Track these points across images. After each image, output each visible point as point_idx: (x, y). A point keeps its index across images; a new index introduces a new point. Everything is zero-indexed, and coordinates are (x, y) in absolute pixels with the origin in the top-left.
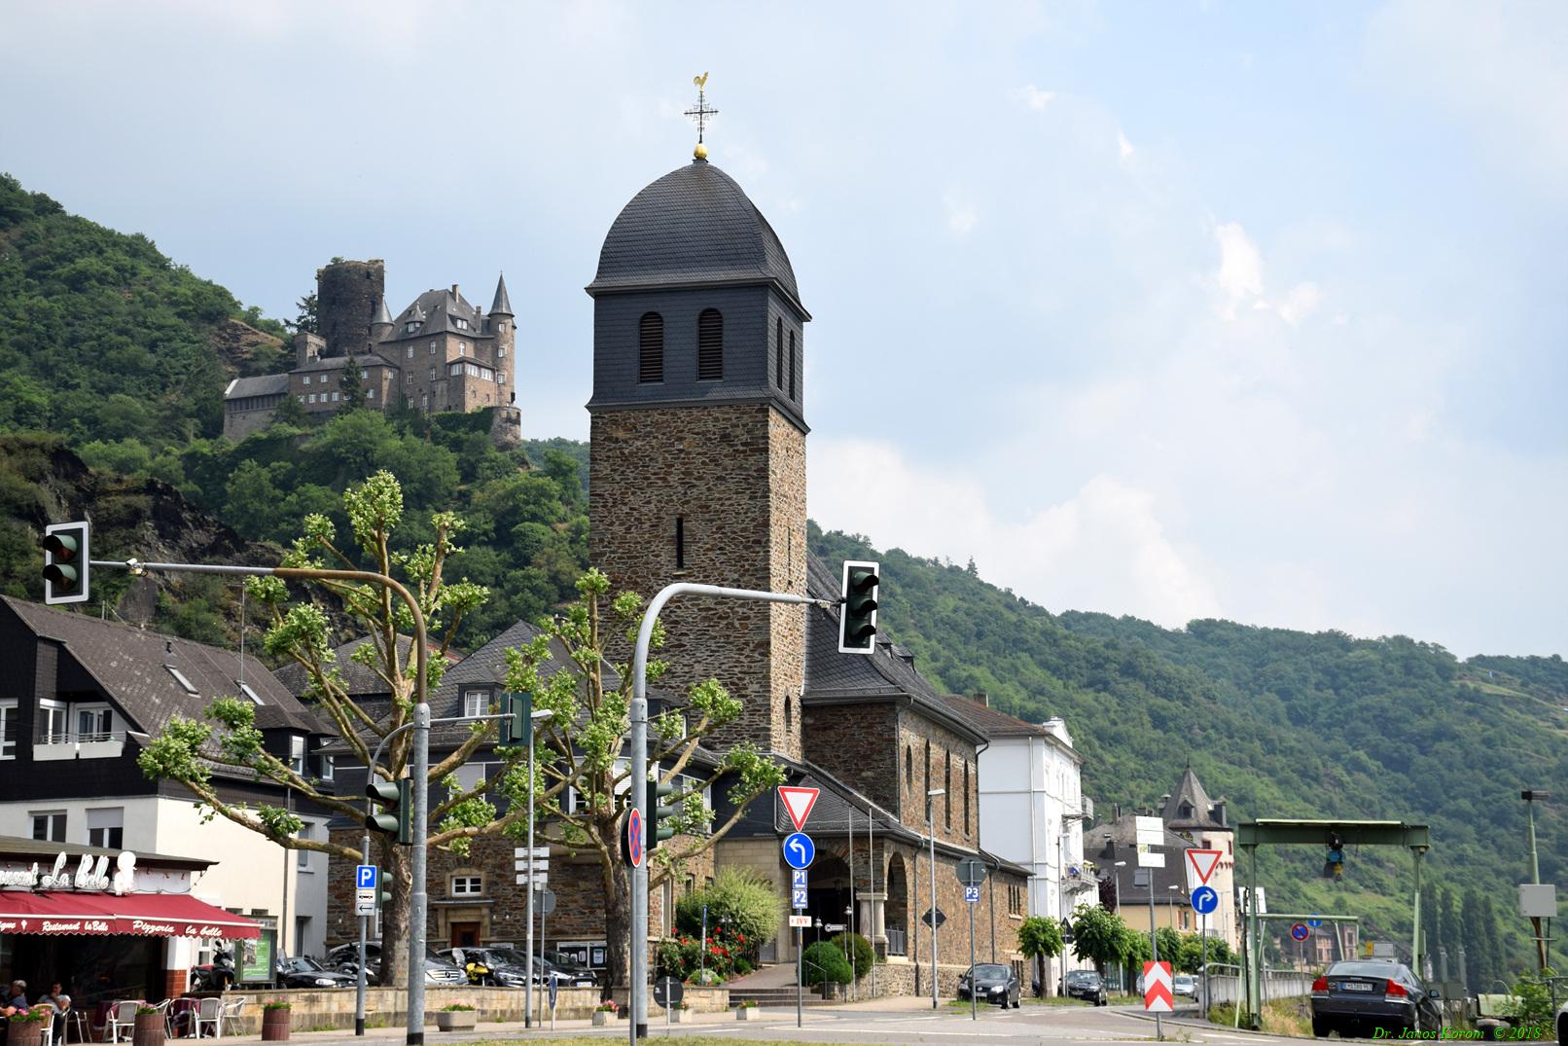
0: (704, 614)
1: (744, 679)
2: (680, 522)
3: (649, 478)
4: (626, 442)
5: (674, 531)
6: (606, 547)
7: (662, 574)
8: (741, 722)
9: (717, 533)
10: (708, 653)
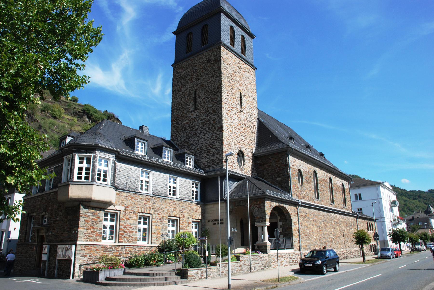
0: (202, 121)
1: (214, 142)
2: (195, 92)
3: (187, 81)
4: (181, 72)
5: (193, 96)
6: (176, 107)
7: (190, 111)
8: (214, 158)
10: (203, 135)
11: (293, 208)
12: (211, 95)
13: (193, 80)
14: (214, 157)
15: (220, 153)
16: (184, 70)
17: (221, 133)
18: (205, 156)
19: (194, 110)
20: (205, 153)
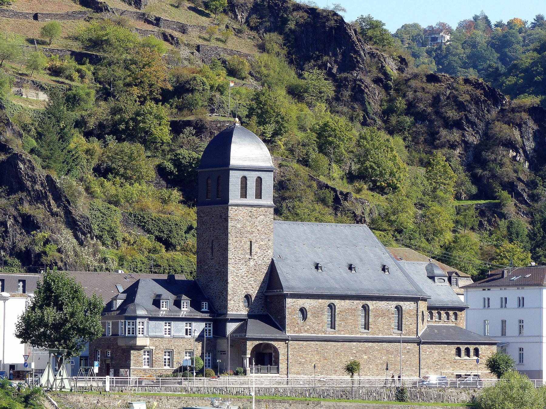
11: (283, 343)
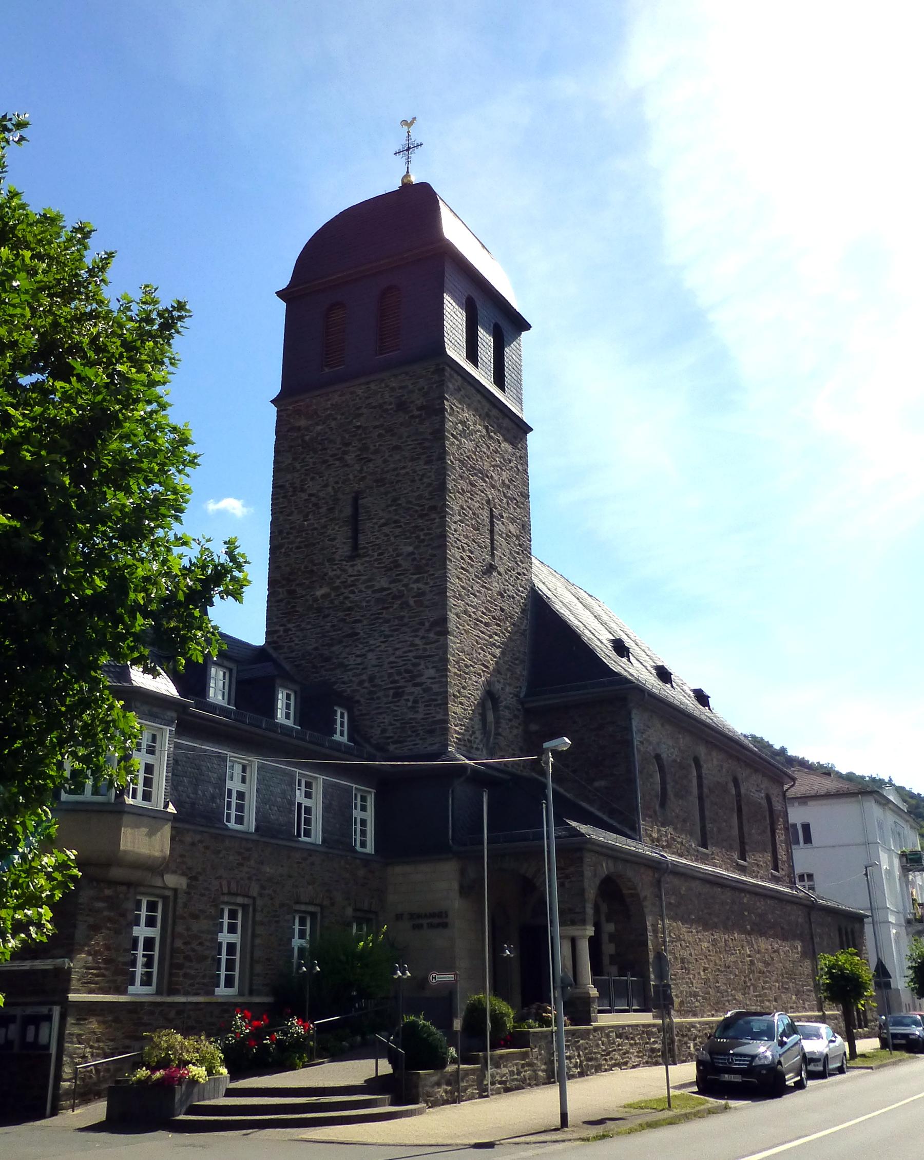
0: (378, 595)
1: (419, 664)
2: (356, 499)
3: (326, 461)
4: (307, 429)
5: (348, 511)
6: (285, 538)
7: (337, 557)
9: (391, 506)
12: (410, 516)
13: (349, 458)
14: (417, 712)
15: (436, 700)
16: (317, 424)
17: (442, 638)
18: (389, 708)
19: (352, 558)
20: (387, 696)
